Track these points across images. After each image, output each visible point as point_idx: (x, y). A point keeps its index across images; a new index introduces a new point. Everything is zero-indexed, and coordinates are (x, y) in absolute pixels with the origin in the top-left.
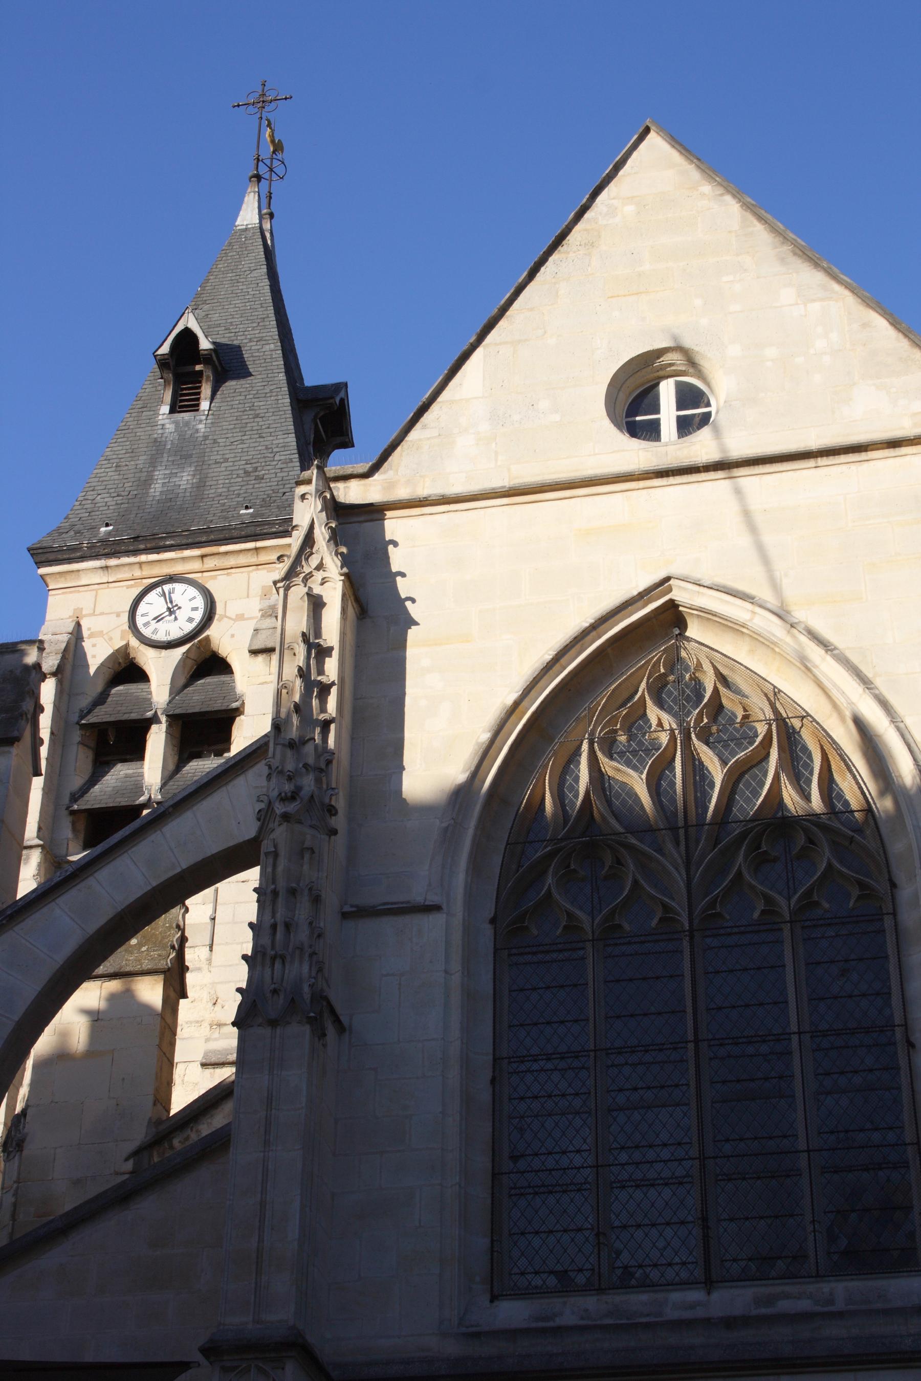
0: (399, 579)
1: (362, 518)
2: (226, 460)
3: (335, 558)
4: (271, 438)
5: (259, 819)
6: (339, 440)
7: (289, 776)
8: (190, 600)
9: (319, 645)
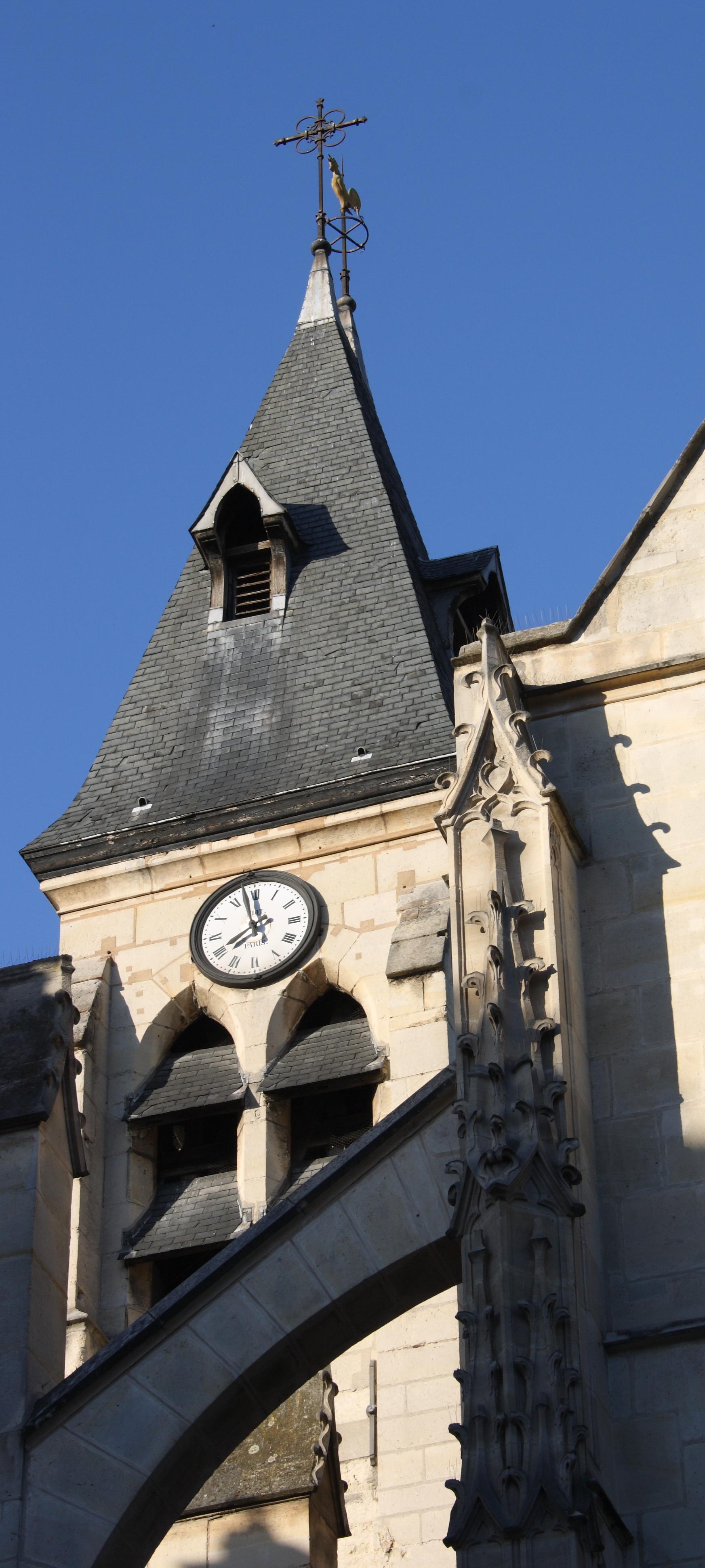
0: (638, 796)
1: (567, 707)
2: (321, 683)
3: (532, 770)
4: (389, 641)
5: (452, 1202)
7: (495, 1124)
8: (286, 907)
9: (521, 911)
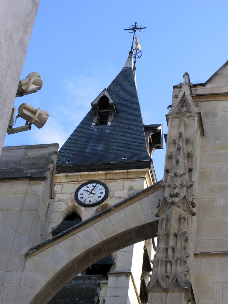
2: (117, 142)
4: (135, 135)
5: (158, 207)
6: (157, 145)
8: (100, 190)
